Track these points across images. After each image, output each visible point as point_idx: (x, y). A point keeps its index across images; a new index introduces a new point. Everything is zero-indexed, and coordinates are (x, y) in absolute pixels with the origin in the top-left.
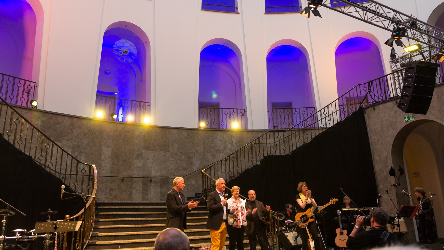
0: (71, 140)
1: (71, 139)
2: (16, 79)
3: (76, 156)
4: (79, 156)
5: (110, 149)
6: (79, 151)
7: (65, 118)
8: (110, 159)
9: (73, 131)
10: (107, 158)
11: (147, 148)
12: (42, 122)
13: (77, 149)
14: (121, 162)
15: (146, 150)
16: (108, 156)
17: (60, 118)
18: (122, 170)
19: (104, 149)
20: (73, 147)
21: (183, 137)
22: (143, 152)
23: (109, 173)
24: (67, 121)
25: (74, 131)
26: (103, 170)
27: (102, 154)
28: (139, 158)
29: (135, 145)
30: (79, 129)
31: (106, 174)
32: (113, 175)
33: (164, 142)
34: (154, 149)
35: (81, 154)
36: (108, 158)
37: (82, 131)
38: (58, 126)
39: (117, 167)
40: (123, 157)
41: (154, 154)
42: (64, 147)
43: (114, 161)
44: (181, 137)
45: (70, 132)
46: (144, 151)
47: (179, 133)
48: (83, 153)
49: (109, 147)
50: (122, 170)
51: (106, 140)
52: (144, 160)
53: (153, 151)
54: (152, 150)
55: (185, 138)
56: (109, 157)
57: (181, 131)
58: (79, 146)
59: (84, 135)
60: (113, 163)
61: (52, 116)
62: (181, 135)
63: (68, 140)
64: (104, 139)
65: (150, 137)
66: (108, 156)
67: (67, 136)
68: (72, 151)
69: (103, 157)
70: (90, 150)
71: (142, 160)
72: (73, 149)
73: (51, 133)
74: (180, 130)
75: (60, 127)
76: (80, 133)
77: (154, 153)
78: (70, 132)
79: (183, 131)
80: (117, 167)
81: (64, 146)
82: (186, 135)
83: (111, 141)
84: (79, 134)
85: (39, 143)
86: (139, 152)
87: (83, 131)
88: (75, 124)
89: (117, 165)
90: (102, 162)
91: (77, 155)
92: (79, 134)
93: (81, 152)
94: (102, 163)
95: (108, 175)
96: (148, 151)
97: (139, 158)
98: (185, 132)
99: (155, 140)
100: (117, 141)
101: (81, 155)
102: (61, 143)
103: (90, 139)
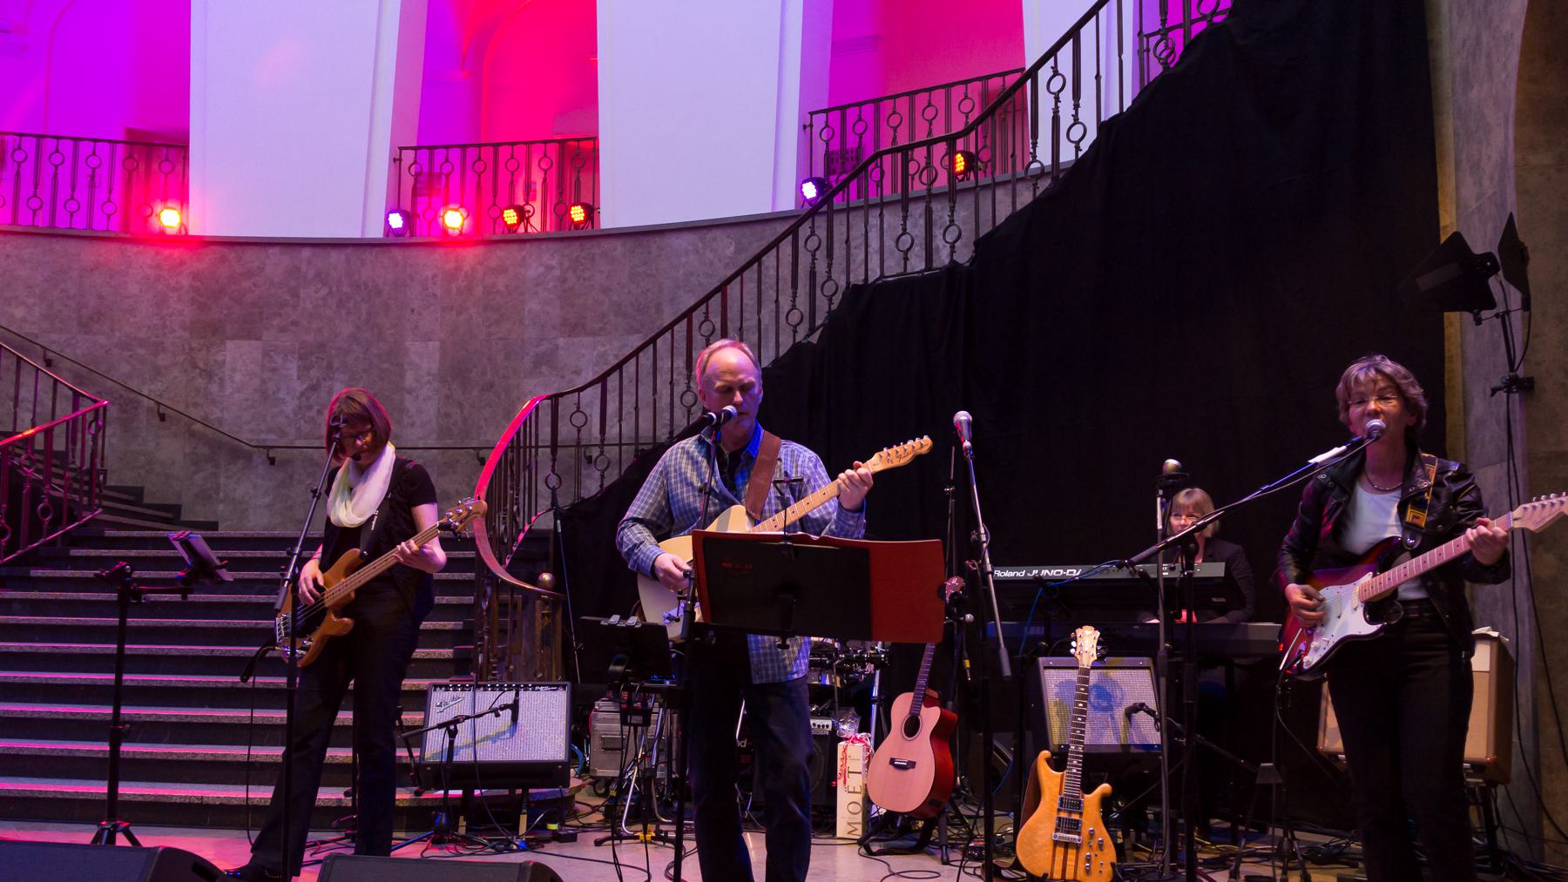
0: (293, 328)
1: (295, 323)
2: (82, 143)
3: (315, 382)
4: (325, 380)
5: (434, 345)
6: (325, 364)
7: (271, 251)
8: (435, 385)
9: (298, 297)
10: (426, 379)
11: (574, 328)
12: (193, 278)
13: (317, 358)
14: (475, 393)
15: (569, 336)
16: (429, 374)
17: (251, 256)
18: (482, 423)
19: (413, 347)
20: (302, 351)
21: (720, 261)
22: (557, 347)
23: (434, 436)
24: (276, 262)
25: (302, 293)
26: (413, 425)
27: (406, 366)
28: (544, 369)
29: (527, 322)
30: (319, 286)
31: (421, 438)
32: (449, 443)
33: (643, 292)
34: (602, 329)
35: (331, 375)
36: (429, 382)
37: (330, 292)
38: (246, 284)
39: (462, 413)
40: (484, 373)
41: (602, 349)
42: (272, 353)
43: (449, 389)
44: (712, 264)
45: (288, 298)
46: (561, 341)
47: (700, 245)
48: (337, 369)
49: (430, 340)
50: (482, 423)
51: (419, 314)
52: (563, 377)
53: (599, 338)
54: (594, 333)
55: (728, 264)
56: (431, 378)
57: (710, 235)
58: (322, 346)
59: (338, 306)
60: (447, 397)
61: (226, 250)
62: (709, 255)
63: (283, 330)
64: (413, 311)
65: (584, 279)
66: (429, 374)
67: (280, 315)
68: (299, 367)
69: (410, 378)
70: (361, 355)
71: (553, 379)
72: (301, 358)
73: (225, 312)
74: (705, 231)
75: (255, 285)
76: (324, 299)
77: (603, 345)
78: (288, 298)
79: (718, 233)
80: (462, 413)
81: (271, 351)
82: (732, 248)
83: (438, 315)
84: (320, 302)
85: (187, 350)
86: (545, 347)
87: (334, 289)
88: (304, 268)
89: (460, 405)
90: (407, 396)
91: (318, 380)
92: (320, 302)
93: (330, 366)
94: (408, 401)
95: (430, 443)
96: (576, 340)
97: (544, 369)
98: (728, 237)
99: (606, 290)
100: (459, 313)
101: (331, 379)
102: (260, 342)
103: (359, 318)
